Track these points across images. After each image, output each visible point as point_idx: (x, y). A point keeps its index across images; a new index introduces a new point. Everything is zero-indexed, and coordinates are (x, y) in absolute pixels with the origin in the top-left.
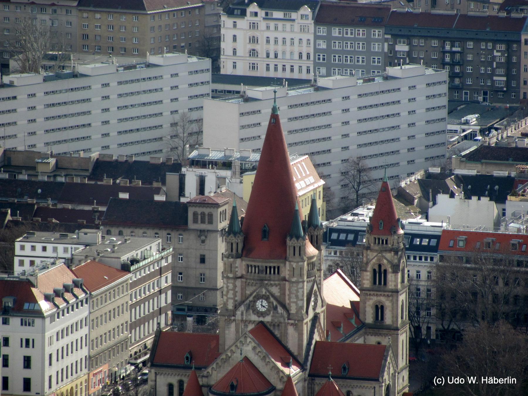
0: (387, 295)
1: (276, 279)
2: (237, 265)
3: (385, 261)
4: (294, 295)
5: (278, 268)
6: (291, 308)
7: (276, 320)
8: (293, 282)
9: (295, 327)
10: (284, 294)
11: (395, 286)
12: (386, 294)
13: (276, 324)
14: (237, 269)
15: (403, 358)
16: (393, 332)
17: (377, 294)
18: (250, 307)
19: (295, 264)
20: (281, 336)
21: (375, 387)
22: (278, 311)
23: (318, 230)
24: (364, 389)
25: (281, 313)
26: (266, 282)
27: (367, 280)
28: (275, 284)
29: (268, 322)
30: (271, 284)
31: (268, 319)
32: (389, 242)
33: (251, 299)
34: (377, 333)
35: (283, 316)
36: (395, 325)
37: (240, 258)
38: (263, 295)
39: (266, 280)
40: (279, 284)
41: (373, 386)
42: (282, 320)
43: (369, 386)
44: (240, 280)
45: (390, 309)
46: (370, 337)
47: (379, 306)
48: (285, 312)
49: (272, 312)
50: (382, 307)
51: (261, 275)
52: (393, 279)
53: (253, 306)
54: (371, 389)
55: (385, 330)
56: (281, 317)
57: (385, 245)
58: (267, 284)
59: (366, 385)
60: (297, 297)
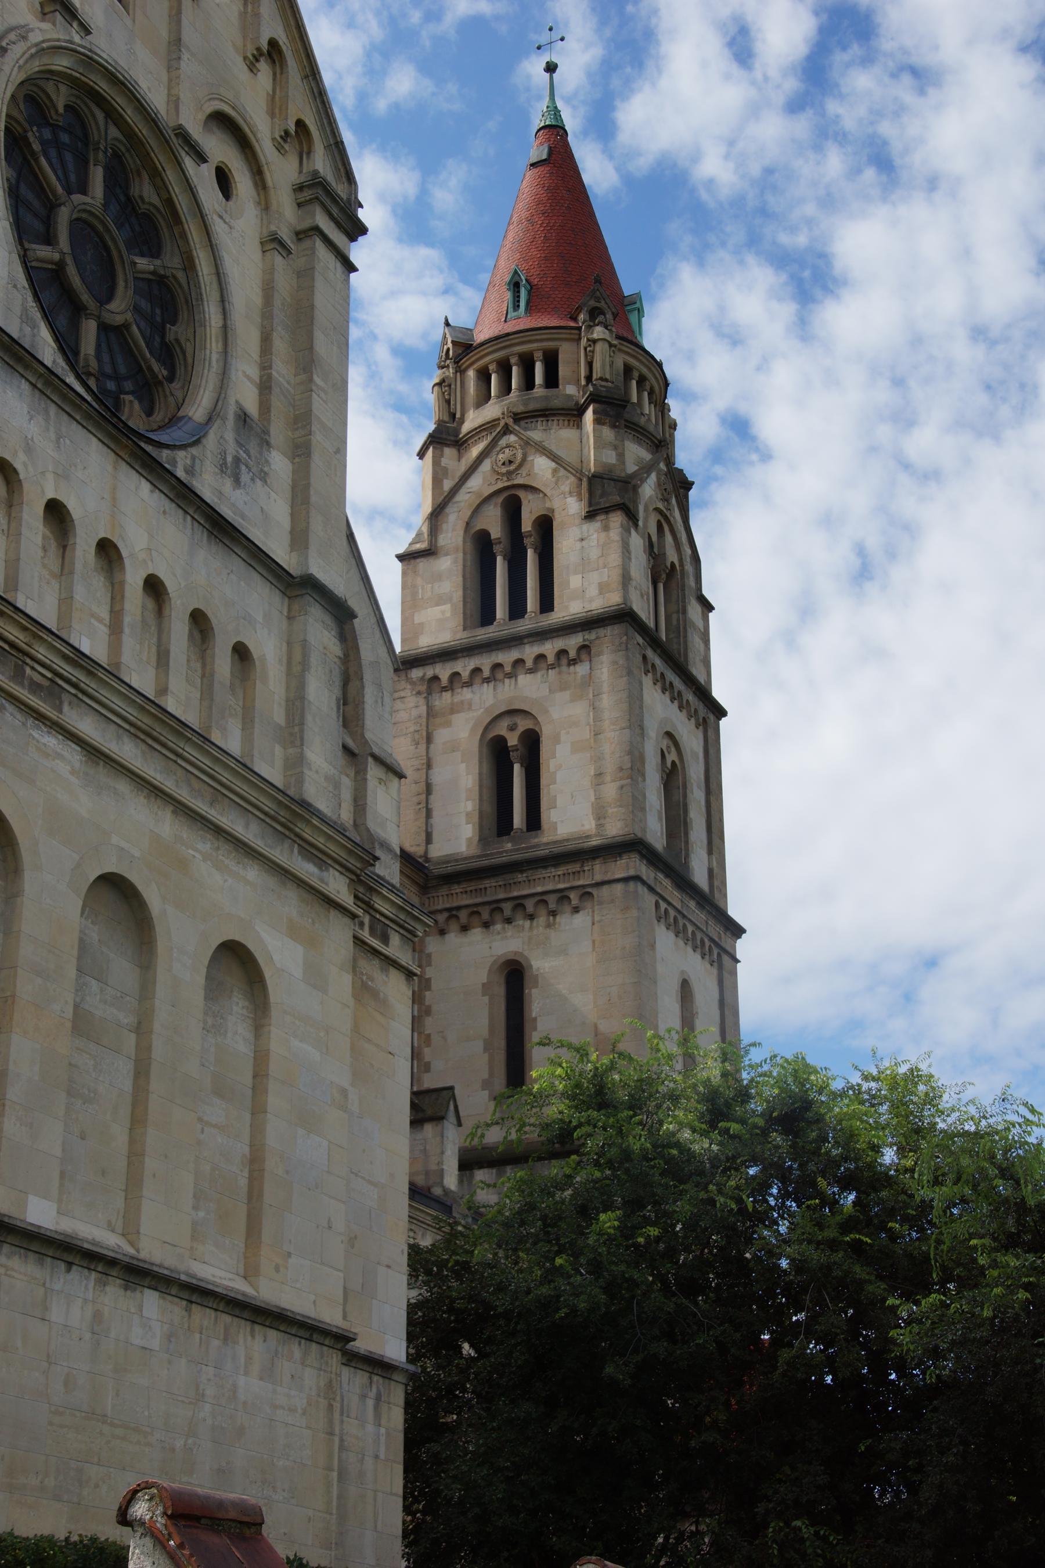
0: (562, 653)
3: (541, 467)
11: (602, 588)
12: (549, 648)
16: (599, 871)
17: (497, 666)
27: (439, 601)
32: (563, 371)
34: (496, 907)
36: (615, 829)
45: (586, 734)
46: (453, 938)
47: (513, 740)
50: (532, 741)
52: (594, 554)
55: (553, 871)
57: (539, 391)
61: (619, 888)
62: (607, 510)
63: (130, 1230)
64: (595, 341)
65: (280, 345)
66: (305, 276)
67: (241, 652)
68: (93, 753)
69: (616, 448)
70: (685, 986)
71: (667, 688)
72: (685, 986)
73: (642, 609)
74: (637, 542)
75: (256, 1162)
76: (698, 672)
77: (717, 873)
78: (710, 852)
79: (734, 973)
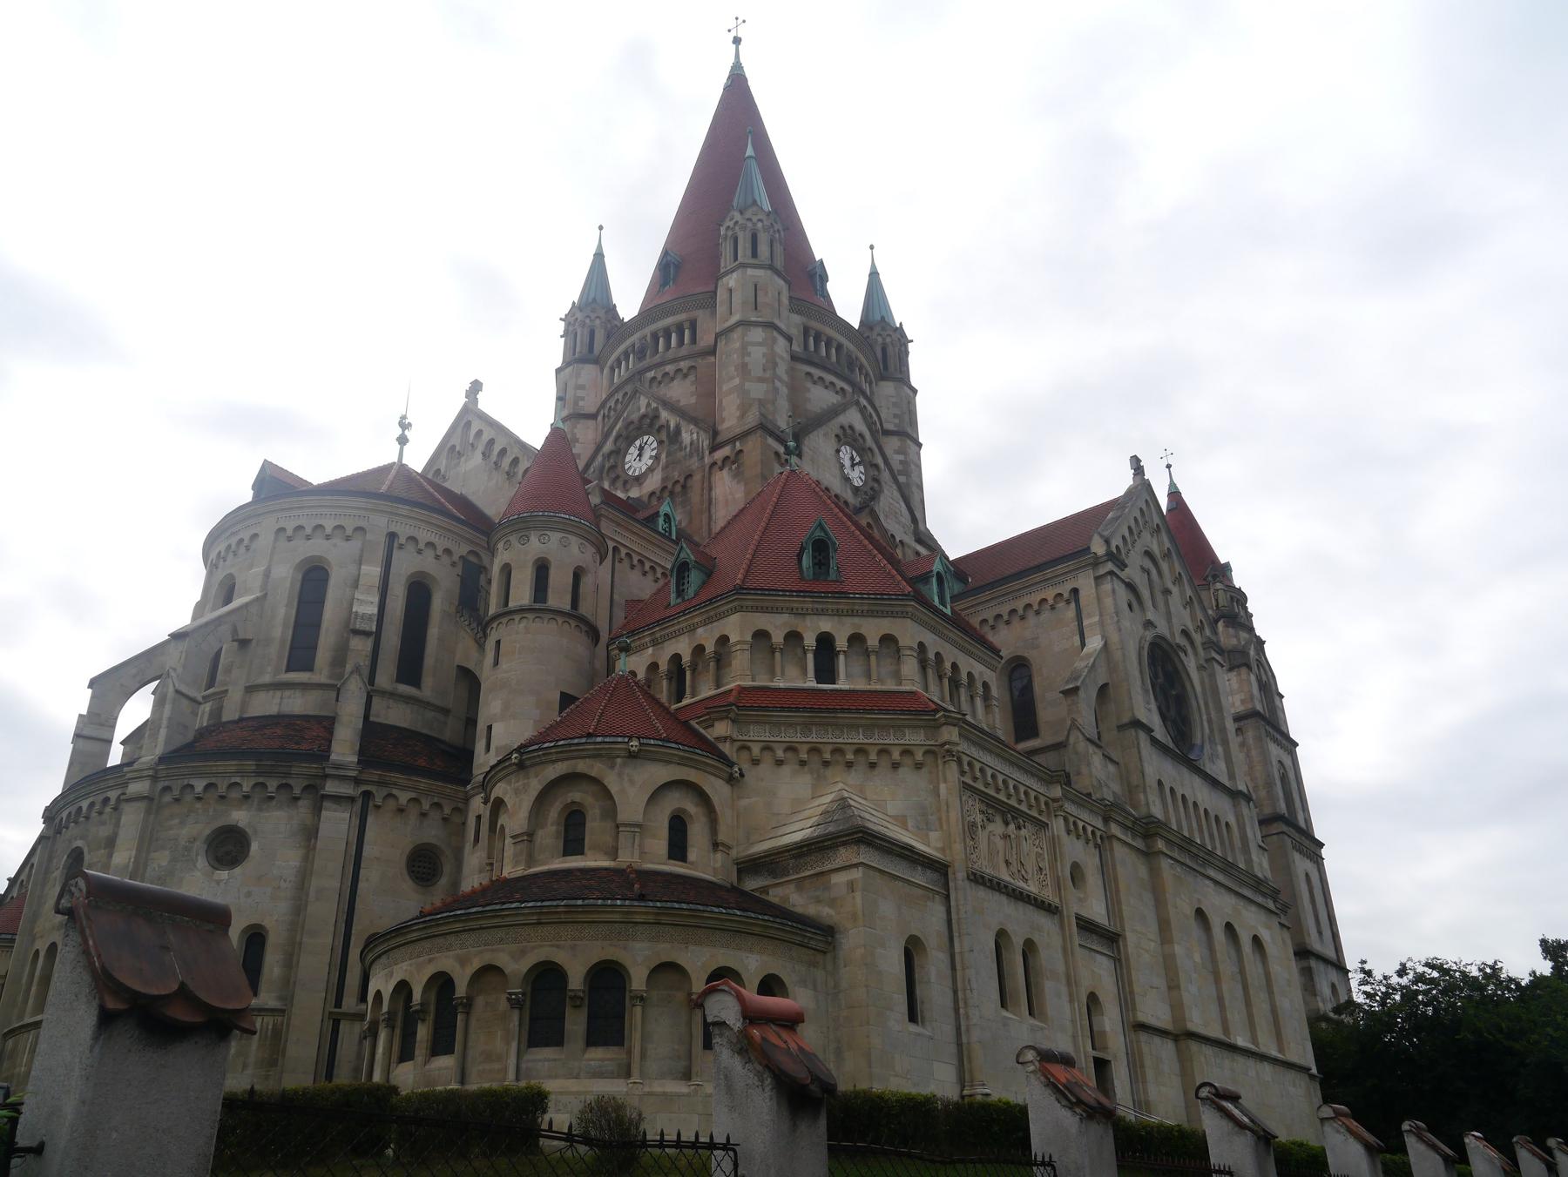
1: (684, 351)
2: (581, 381)
4: (733, 369)
5: (693, 325)
6: (725, 414)
7: (676, 478)
8: (731, 329)
9: (734, 467)
10: (708, 393)
11: (1243, 702)
13: (678, 488)
14: (580, 393)
15: (1320, 933)
18: (604, 475)
19: (735, 275)
20: (690, 522)
21: (1075, 591)
22: (682, 442)
23: (883, 329)
24: (1032, 619)
25: (691, 444)
26: (651, 374)
28: (679, 370)
29: (653, 493)
30: (666, 374)
31: (653, 483)
33: (609, 446)
35: (697, 450)
37: (596, 361)
38: (644, 416)
39: (649, 369)
40: (693, 367)
41: (1065, 589)
42: (694, 463)
43: (1049, 594)
44: (591, 423)
48: (702, 433)
49: (663, 456)
51: (641, 364)
52: (1235, 686)
53: (613, 467)
54: (1061, 605)
56: (691, 455)
58: (654, 378)
59: (1034, 599)
60: (744, 369)
61: (1275, 837)
62: (1238, 667)
63: (1254, 1040)
64: (1218, 590)
65: (1211, 705)
66: (1212, 676)
67: (1227, 824)
68: (1216, 882)
69: (1236, 637)
70: (1307, 875)
71: (1275, 741)
72: (1307, 875)
73: (1259, 707)
74: (1253, 678)
75: (1274, 1011)
76: (1283, 728)
77: (1308, 821)
78: (1304, 811)
79: (1323, 865)
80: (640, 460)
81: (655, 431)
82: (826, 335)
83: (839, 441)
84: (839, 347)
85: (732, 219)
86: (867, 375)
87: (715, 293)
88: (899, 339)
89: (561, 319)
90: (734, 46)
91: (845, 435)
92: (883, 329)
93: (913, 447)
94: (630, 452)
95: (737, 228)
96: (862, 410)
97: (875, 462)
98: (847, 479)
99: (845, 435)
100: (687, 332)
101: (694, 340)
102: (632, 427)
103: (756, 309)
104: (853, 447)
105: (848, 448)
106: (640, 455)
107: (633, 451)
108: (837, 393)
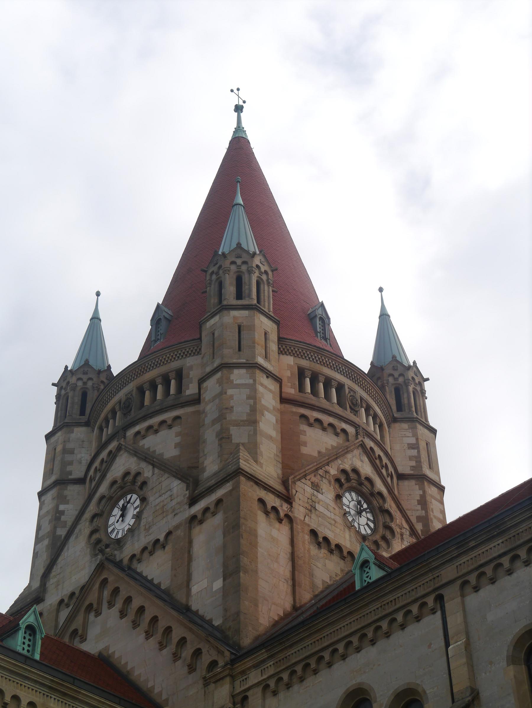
33: (92, 508)
37: (87, 424)
58: (138, 433)
80: (122, 521)
81: (137, 488)
82: (335, 380)
83: (341, 485)
84: (340, 388)
85: (217, 264)
86: (375, 417)
87: (200, 339)
88: (413, 378)
89: (53, 384)
90: (236, 113)
91: (348, 479)
92: (395, 369)
93: (432, 491)
94: (113, 513)
95: (221, 272)
96: (369, 453)
97: (386, 506)
98: (350, 526)
99: (348, 479)
100: (173, 382)
101: (180, 389)
102: (115, 487)
103: (240, 350)
104: (359, 493)
105: (353, 494)
106: (123, 516)
107: (117, 512)
108: (337, 434)
